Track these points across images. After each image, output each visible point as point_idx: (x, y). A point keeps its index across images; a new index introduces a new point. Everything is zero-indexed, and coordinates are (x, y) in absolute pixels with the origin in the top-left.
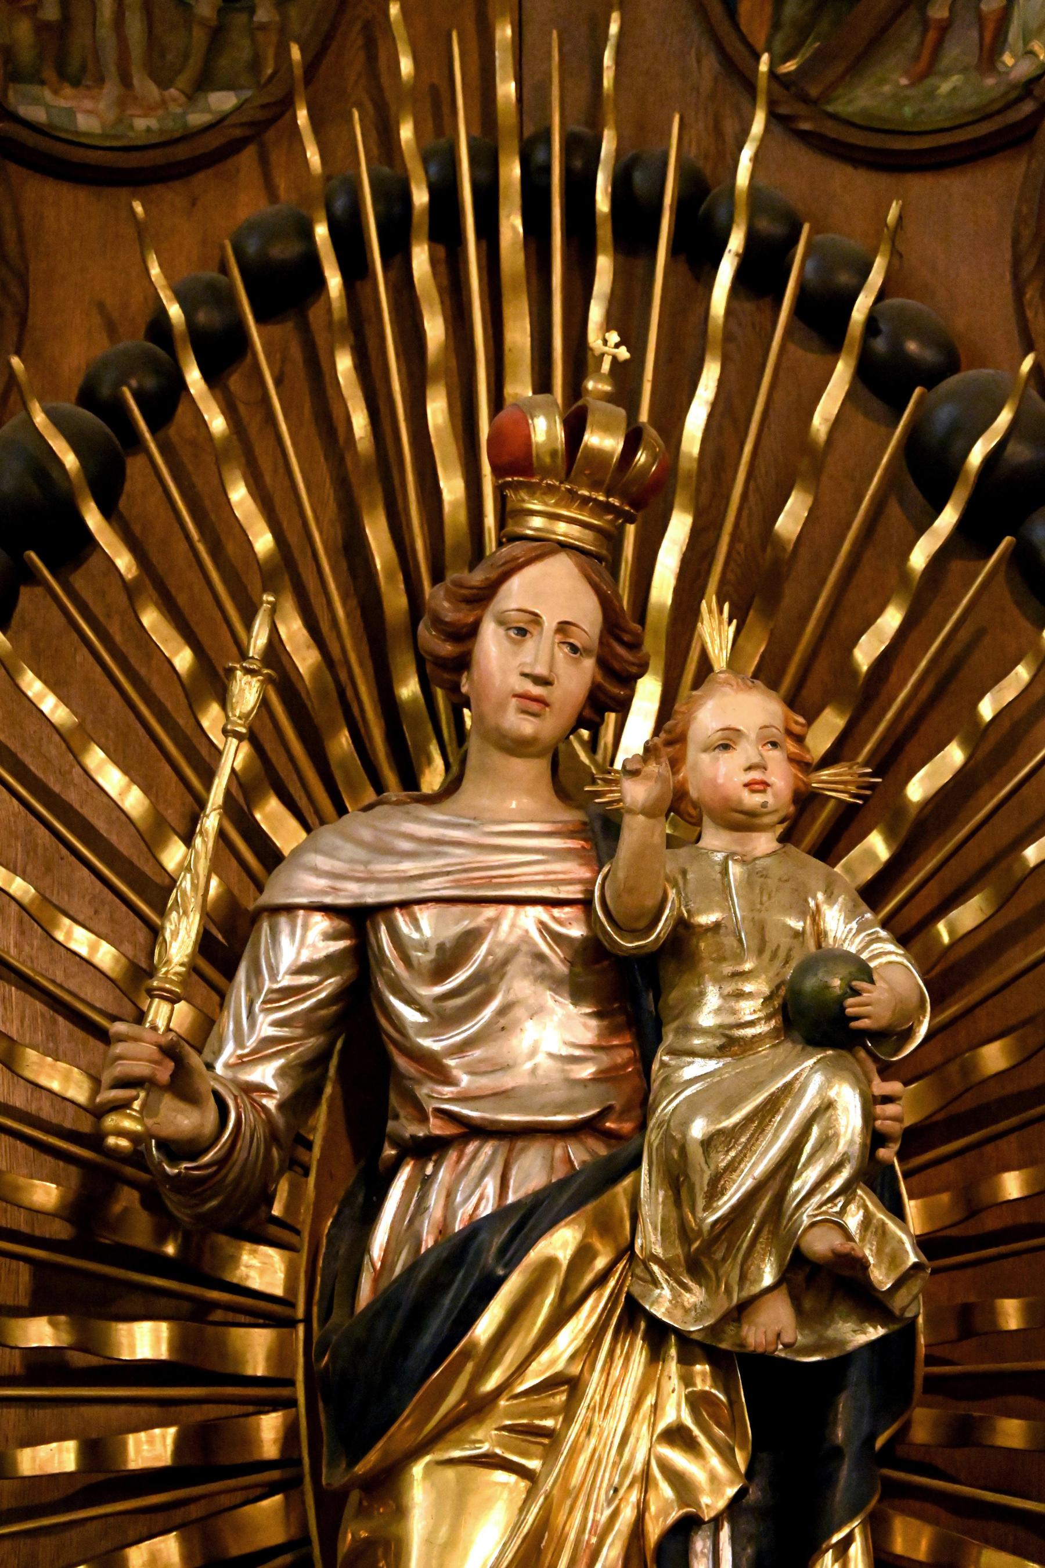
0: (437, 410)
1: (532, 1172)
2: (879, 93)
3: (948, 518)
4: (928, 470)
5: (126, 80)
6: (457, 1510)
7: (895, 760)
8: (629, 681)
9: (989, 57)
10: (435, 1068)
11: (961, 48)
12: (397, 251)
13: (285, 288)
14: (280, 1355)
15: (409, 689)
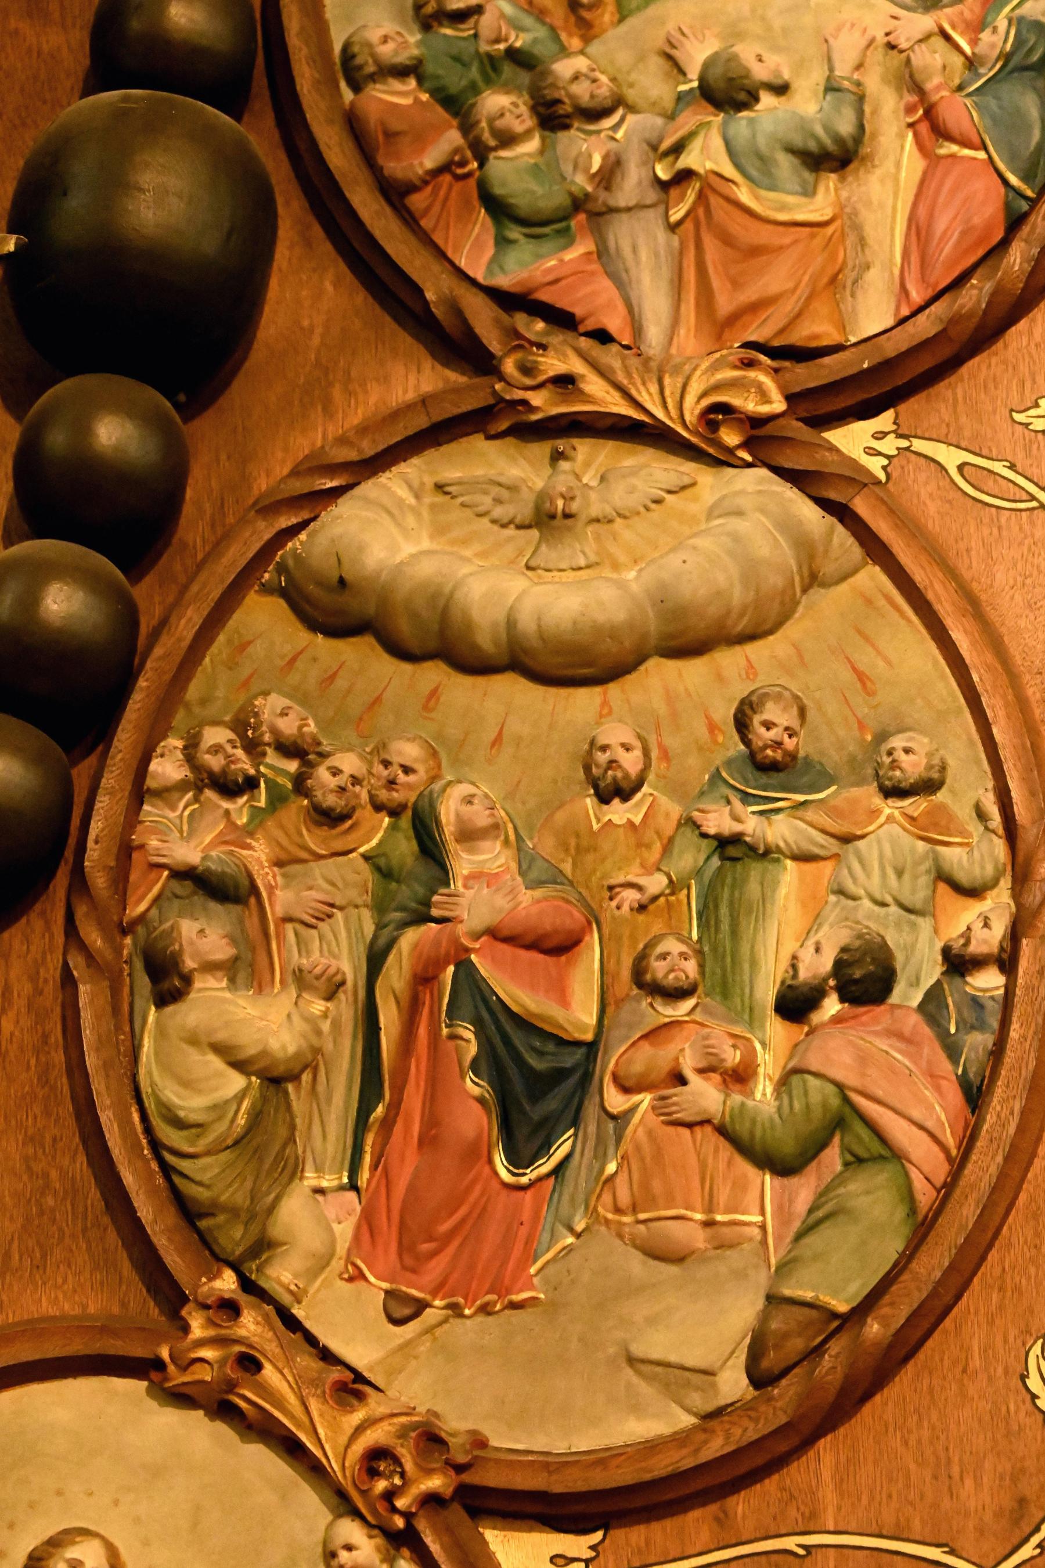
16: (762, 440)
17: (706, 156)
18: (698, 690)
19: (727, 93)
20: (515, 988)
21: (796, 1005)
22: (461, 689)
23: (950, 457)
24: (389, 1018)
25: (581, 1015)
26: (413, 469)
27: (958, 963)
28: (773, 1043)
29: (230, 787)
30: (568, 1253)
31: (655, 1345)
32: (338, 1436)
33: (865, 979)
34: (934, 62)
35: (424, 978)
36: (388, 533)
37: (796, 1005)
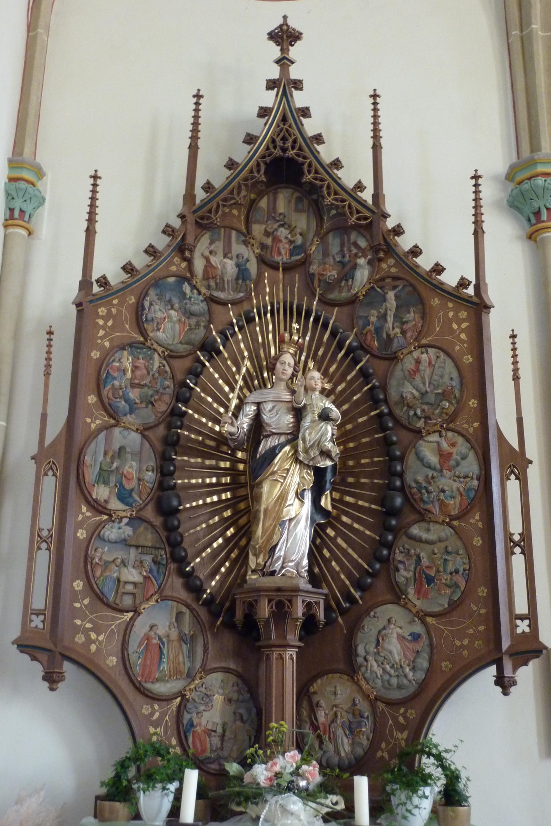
0: (270, 336)
1: (283, 439)
2: (333, 296)
3: (343, 352)
4: (340, 346)
5: (229, 291)
6: (272, 488)
7: (336, 385)
8: (297, 372)
9: (349, 290)
10: (268, 425)
11: (345, 289)
12: (265, 315)
13: (250, 320)
14: (245, 467)
15: (265, 375)
16: (448, 524)
17: (442, 497)
18: (443, 545)
19: (443, 491)
20: (428, 572)
21: (451, 573)
22: (422, 545)
23: (463, 524)
24: (417, 575)
25: (433, 574)
26: (417, 524)
27: (464, 570)
28: (449, 577)
29: (402, 552)
30: (432, 594)
31: (440, 602)
32: (414, 610)
33: (457, 572)
34: (462, 489)
35: (420, 571)
36: (415, 530)
37: (451, 573)
